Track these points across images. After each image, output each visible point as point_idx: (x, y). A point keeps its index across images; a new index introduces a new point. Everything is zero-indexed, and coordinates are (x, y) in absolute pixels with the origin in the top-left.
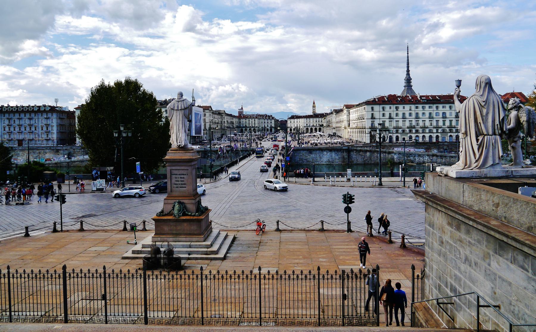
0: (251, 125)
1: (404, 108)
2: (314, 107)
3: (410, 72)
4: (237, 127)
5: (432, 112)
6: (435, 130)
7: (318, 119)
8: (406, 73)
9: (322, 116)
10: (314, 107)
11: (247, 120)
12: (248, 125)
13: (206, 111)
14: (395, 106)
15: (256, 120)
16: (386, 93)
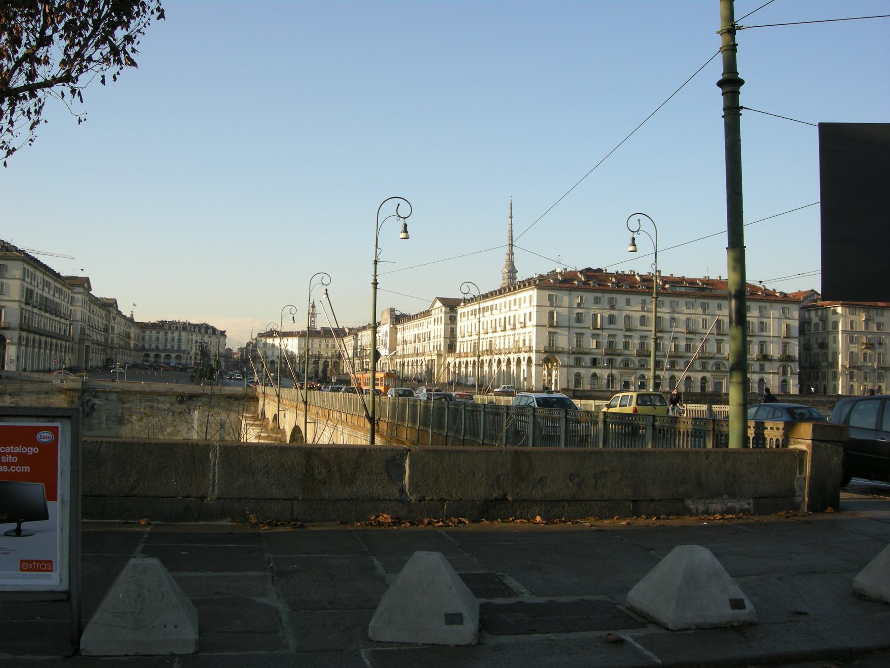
0: (169, 347)
1: (628, 303)
2: (312, 315)
3: (515, 258)
4: (136, 349)
5: (693, 317)
6: (697, 366)
7: (330, 341)
8: (506, 257)
9: (340, 333)
10: (312, 315)
11: (162, 333)
12: (161, 347)
13: (77, 289)
14: (607, 296)
15: (184, 334)
16: (577, 263)
